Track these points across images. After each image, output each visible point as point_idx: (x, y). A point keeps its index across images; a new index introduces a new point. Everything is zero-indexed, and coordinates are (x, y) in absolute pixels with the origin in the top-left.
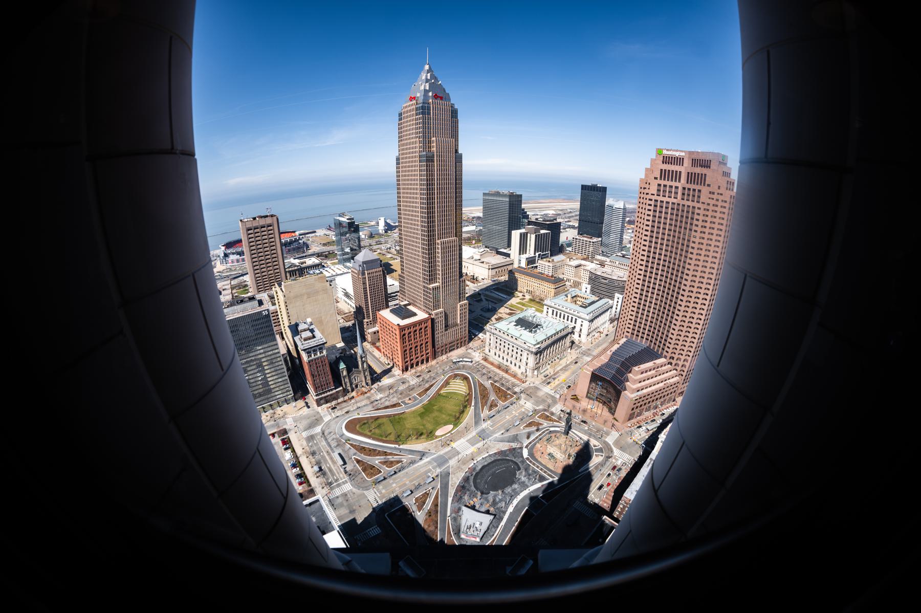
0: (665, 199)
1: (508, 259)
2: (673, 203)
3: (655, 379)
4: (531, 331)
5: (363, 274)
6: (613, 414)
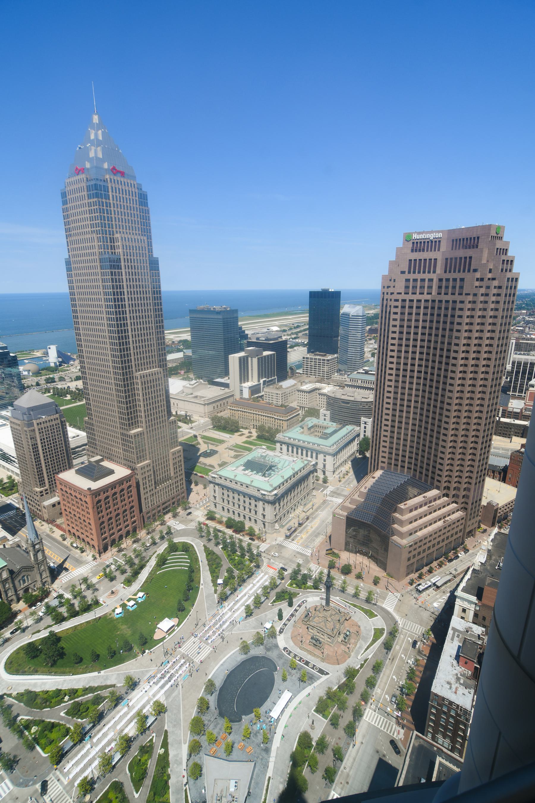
0: (415, 297)
1: (227, 390)
2: (426, 301)
3: (429, 517)
4: (264, 475)
5: (31, 425)
6: (385, 569)
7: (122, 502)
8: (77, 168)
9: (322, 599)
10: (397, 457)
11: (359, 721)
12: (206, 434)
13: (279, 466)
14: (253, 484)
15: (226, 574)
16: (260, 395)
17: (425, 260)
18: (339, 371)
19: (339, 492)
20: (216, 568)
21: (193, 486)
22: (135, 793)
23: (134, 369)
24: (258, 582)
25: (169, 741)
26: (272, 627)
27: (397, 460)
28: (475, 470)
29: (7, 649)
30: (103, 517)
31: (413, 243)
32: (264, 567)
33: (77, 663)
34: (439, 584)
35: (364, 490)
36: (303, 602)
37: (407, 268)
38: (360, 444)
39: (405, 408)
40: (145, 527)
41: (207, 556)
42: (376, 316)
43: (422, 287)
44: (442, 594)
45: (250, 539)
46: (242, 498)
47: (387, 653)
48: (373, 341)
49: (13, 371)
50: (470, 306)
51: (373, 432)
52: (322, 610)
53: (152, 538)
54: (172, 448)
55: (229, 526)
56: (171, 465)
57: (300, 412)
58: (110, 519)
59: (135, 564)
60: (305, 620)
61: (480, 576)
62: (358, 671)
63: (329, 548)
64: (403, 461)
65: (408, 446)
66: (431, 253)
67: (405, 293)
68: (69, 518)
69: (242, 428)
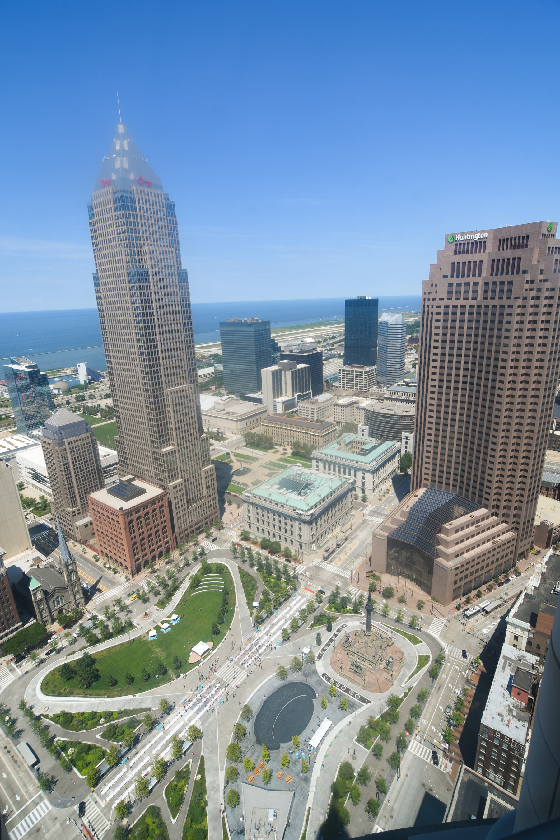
0: (459, 303)
1: (260, 405)
2: (471, 306)
3: (477, 538)
4: (300, 494)
5: (61, 444)
6: (429, 593)
7: (154, 522)
8: (103, 181)
9: (362, 623)
10: (441, 474)
11: (404, 752)
12: (239, 451)
13: (316, 484)
14: (288, 503)
15: (262, 597)
16: (294, 410)
17: (470, 262)
18: (378, 383)
19: (380, 512)
20: (251, 590)
21: (226, 505)
22: (172, 818)
23: (164, 385)
24: (295, 605)
25: (205, 767)
26: (310, 652)
27: (441, 477)
28: (527, 487)
29: (43, 670)
30: (135, 537)
31: (456, 245)
32: (301, 589)
33: (112, 686)
34: (488, 609)
35: (406, 509)
36: (342, 626)
37: (450, 272)
38: (402, 460)
39: (449, 421)
40: (177, 547)
41: (242, 578)
42: (416, 324)
43: (467, 292)
44: (491, 619)
45: (286, 560)
46: (277, 517)
47: (432, 682)
48: (413, 351)
49: (44, 389)
50: (519, 310)
51: (415, 447)
52: (362, 635)
53: (185, 559)
54: (205, 466)
55: (264, 547)
56: (204, 484)
57: (337, 427)
58: (143, 539)
59: (168, 585)
60: (345, 645)
61: (534, 601)
62: (402, 700)
63: (369, 570)
64: (448, 479)
65: (453, 462)
66: (476, 255)
67: (448, 299)
68: (101, 538)
69: (277, 444)
